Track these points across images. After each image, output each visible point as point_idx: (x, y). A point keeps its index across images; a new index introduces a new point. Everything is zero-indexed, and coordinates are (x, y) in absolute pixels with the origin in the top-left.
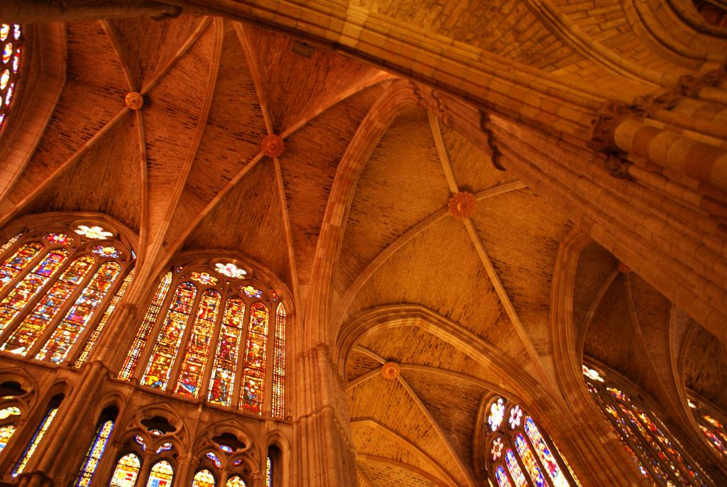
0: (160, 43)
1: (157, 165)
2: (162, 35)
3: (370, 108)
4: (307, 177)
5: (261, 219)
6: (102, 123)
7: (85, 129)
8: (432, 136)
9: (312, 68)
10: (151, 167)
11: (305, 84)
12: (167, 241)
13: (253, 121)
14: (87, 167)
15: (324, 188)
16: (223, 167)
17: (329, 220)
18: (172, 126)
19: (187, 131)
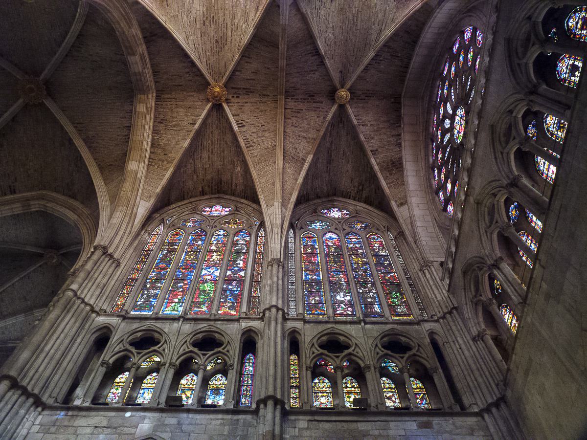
0: (331, 147)
1: (310, 53)
2: (331, 153)
3: (148, 171)
4: (178, 75)
5: (204, 21)
6: (366, 69)
7: (379, 63)
8: (90, 150)
9: (208, 166)
10: (315, 50)
11: (209, 151)
12: (277, 8)
13: (241, 109)
14: (373, 27)
15: (159, 72)
16: (253, 65)
17: (142, 56)
18: (305, 84)
19: (292, 85)
